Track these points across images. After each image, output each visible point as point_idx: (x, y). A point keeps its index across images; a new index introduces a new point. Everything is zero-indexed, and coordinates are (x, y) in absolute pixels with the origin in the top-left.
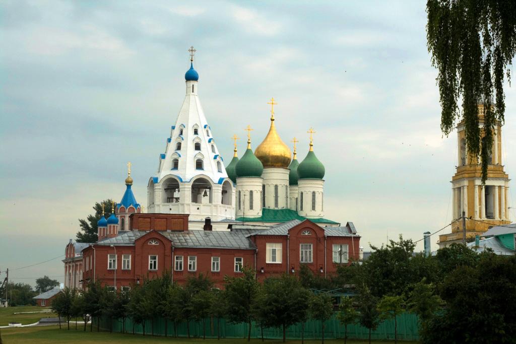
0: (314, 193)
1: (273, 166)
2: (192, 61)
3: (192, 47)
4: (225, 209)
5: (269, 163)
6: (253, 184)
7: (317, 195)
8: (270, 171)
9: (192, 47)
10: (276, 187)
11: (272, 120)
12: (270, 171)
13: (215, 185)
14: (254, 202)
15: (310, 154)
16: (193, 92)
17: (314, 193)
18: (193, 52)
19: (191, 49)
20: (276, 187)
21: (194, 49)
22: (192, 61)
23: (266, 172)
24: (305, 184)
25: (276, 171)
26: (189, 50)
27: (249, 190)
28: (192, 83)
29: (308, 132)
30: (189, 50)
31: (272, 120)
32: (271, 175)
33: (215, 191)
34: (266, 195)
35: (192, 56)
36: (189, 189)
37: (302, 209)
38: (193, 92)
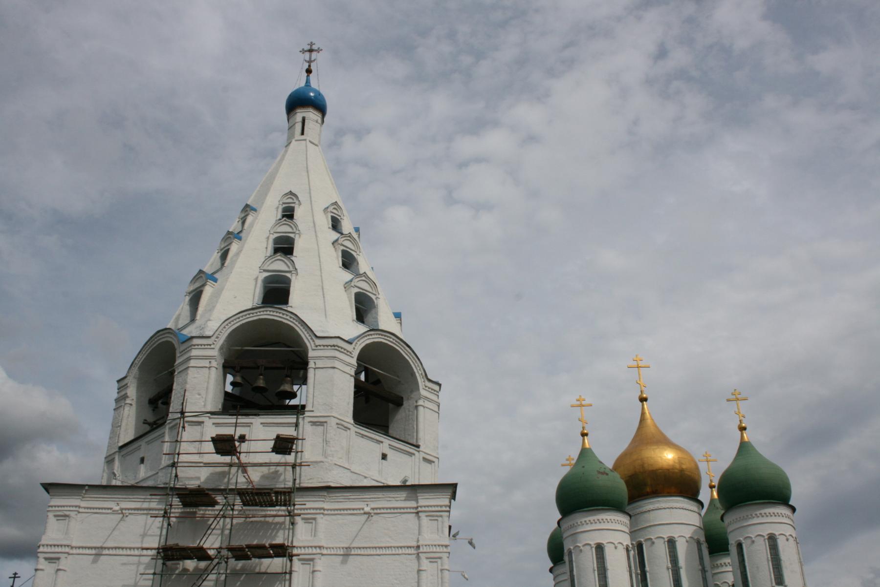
1: (656, 493)
2: (309, 71)
3: (311, 44)
4: (378, 450)
5: (648, 489)
6: (598, 526)
8: (651, 507)
9: (311, 44)
12: (651, 507)
13: (318, 342)
14: (610, 574)
15: (744, 447)
16: (303, 133)
18: (314, 55)
19: (307, 48)
20: (671, 543)
21: (314, 47)
22: (309, 71)
25: (663, 505)
26: (303, 51)
28: (300, 114)
29: (728, 400)
30: (303, 51)
32: (652, 515)
33: (320, 364)
34: (647, 568)
35: (310, 62)
36: (205, 363)
38: (303, 133)
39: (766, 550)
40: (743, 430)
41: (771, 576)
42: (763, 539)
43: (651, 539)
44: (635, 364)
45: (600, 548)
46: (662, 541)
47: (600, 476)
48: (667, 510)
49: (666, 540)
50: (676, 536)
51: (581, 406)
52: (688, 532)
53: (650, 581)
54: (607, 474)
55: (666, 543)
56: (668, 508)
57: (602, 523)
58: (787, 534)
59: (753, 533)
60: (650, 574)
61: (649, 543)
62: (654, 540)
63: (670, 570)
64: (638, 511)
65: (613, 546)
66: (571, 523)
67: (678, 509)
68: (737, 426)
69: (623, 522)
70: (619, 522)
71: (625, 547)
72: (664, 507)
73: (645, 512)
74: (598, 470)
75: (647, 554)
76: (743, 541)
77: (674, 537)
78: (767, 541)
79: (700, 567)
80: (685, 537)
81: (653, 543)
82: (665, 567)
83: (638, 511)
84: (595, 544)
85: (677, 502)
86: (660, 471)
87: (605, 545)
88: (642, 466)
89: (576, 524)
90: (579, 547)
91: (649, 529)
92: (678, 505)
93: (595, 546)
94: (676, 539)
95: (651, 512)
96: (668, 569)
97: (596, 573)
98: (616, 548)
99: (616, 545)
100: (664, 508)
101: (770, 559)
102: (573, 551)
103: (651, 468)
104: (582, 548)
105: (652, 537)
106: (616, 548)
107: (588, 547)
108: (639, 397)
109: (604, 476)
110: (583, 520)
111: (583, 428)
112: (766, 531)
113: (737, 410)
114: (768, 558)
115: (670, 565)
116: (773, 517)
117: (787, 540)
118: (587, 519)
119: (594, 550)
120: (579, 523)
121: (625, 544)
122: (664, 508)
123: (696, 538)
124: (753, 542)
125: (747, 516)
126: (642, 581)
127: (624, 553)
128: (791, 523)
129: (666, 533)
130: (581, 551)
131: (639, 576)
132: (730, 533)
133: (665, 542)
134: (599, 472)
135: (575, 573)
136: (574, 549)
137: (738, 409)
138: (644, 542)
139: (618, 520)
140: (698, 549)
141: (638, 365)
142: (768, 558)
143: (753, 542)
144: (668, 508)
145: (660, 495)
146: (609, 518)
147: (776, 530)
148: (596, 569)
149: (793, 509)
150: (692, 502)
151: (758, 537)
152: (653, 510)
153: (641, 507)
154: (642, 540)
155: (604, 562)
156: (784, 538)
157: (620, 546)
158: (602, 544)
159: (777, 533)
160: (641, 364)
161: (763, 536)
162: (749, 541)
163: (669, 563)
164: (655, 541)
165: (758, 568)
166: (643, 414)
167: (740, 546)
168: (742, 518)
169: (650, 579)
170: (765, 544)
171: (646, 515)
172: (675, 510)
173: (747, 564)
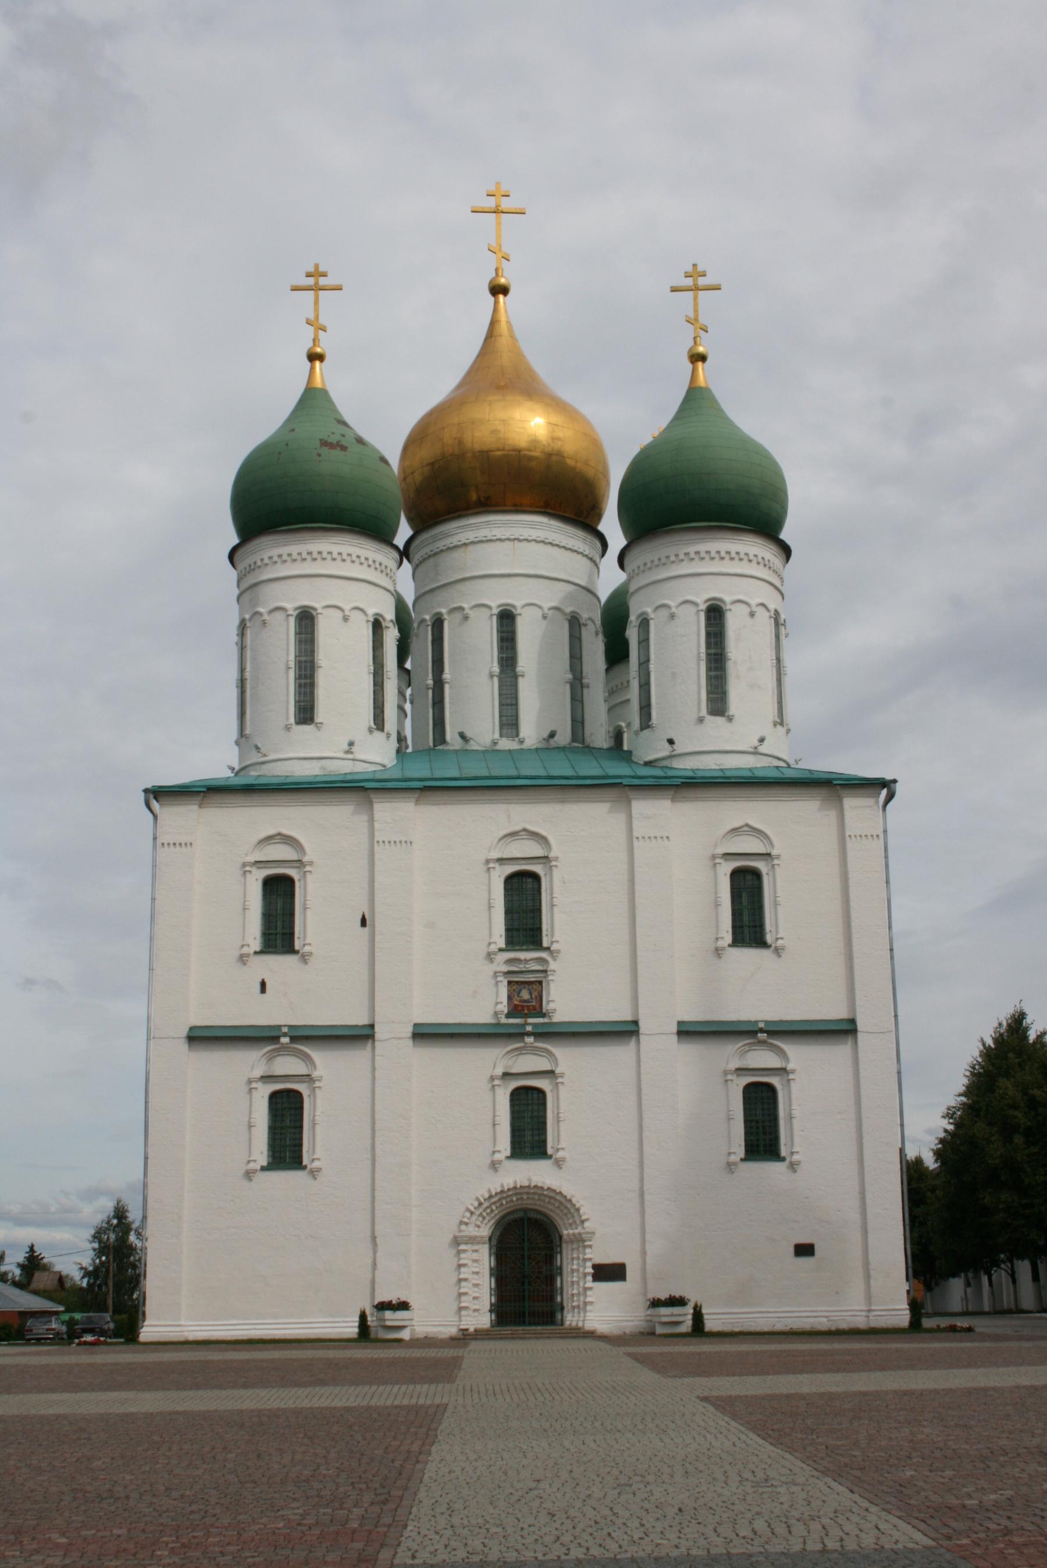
0: (715, 614)
1: (487, 505)
6: (308, 568)
7: (734, 622)
8: (470, 536)
10: (507, 618)
11: (498, 290)
12: (470, 536)
14: (322, 678)
17: (715, 614)
20: (507, 618)
23: (454, 541)
24: (662, 564)
25: (498, 533)
27: (290, 606)
31: (498, 290)
34: (447, 676)
37: (646, 722)
39: (699, 635)
40: (697, 361)
41: (699, 693)
42: (692, 609)
43: (461, 609)
44: (491, 203)
45: (306, 619)
46: (486, 612)
47: (325, 451)
48: (507, 542)
49: (496, 611)
50: (518, 604)
51: (317, 288)
52: (550, 596)
53: (451, 703)
54: (344, 448)
55: (495, 618)
56: (509, 539)
57: (319, 560)
58: (753, 602)
59: (673, 595)
60: (451, 687)
61: (458, 616)
62: (467, 611)
63: (496, 680)
64: (441, 545)
65: (339, 614)
66: (250, 560)
67: (533, 543)
68: (687, 350)
69: (374, 562)
70: (371, 562)
71: (372, 620)
72: (498, 537)
73: (456, 547)
74: (326, 438)
75: (449, 643)
76: (652, 616)
77: (514, 607)
78: (702, 616)
79: (570, 676)
80: (540, 607)
81: (466, 618)
82: (487, 672)
83: (441, 545)
84: (296, 609)
85: (532, 526)
86: (499, 453)
87: (319, 611)
88: (461, 442)
89: (259, 563)
90: (261, 614)
91: (459, 586)
92: (534, 534)
93: (295, 613)
94: (519, 611)
95: (470, 548)
96: (492, 676)
97: (292, 674)
98: (346, 619)
99: (347, 613)
100: (500, 540)
101: (703, 656)
102: (248, 625)
103: (477, 447)
104: (266, 617)
105: (465, 606)
106: (346, 619)
107: (279, 616)
108: (491, 282)
109: (337, 453)
110: (275, 552)
111: (315, 341)
112: (703, 593)
113: (692, 315)
114: (699, 653)
115: (496, 669)
116: (727, 561)
117: (752, 615)
118: (284, 550)
119: (292, 621)
120: (266, 561)
121: (371, 611)
122: (500, 540)
123: (568, 610)
124: (672, 616)
125: (668, 557)
126: (434, 704)
127: (368, 632)
128: (778, 584)
129: (496, 597)
130: (264, 623)
131: (430, 692)
132: (633, 593)
133: (492, 615)
134: (324, 443)
135: (247, 675)
136: (251, 619)
137: (696, 311)
138: (446, 616)
139: (374, 562)
140: (572, 636)
141: (497, 206)
142: (699, 653)
143: (672, 616)
144: (509, 539)
145: (498, 508)
146: (335, 549)
147: (725, 592)
148: (292, 664)
149: (786, 551)
150: (580, 533)
151: (684, 606)
152: (473, 543)
153: (448, 535)
154: (444, 611)
155: (312, 652)
156: (746, 610)
157: (356, 616)
158: (315, 609)
159: (728, 599)
160: (505, 204)
161: (695, 604)
162: (664, 613)
163: (496, 664)
164: (471, 613)
165: (674, 674)
166: (494, 323)
167: (644, 623)
168: (656, 562)
169: (450, 698)
170: (699, 622)
171: (457, 554)
172: (525, 544)
173: (652, 667)
